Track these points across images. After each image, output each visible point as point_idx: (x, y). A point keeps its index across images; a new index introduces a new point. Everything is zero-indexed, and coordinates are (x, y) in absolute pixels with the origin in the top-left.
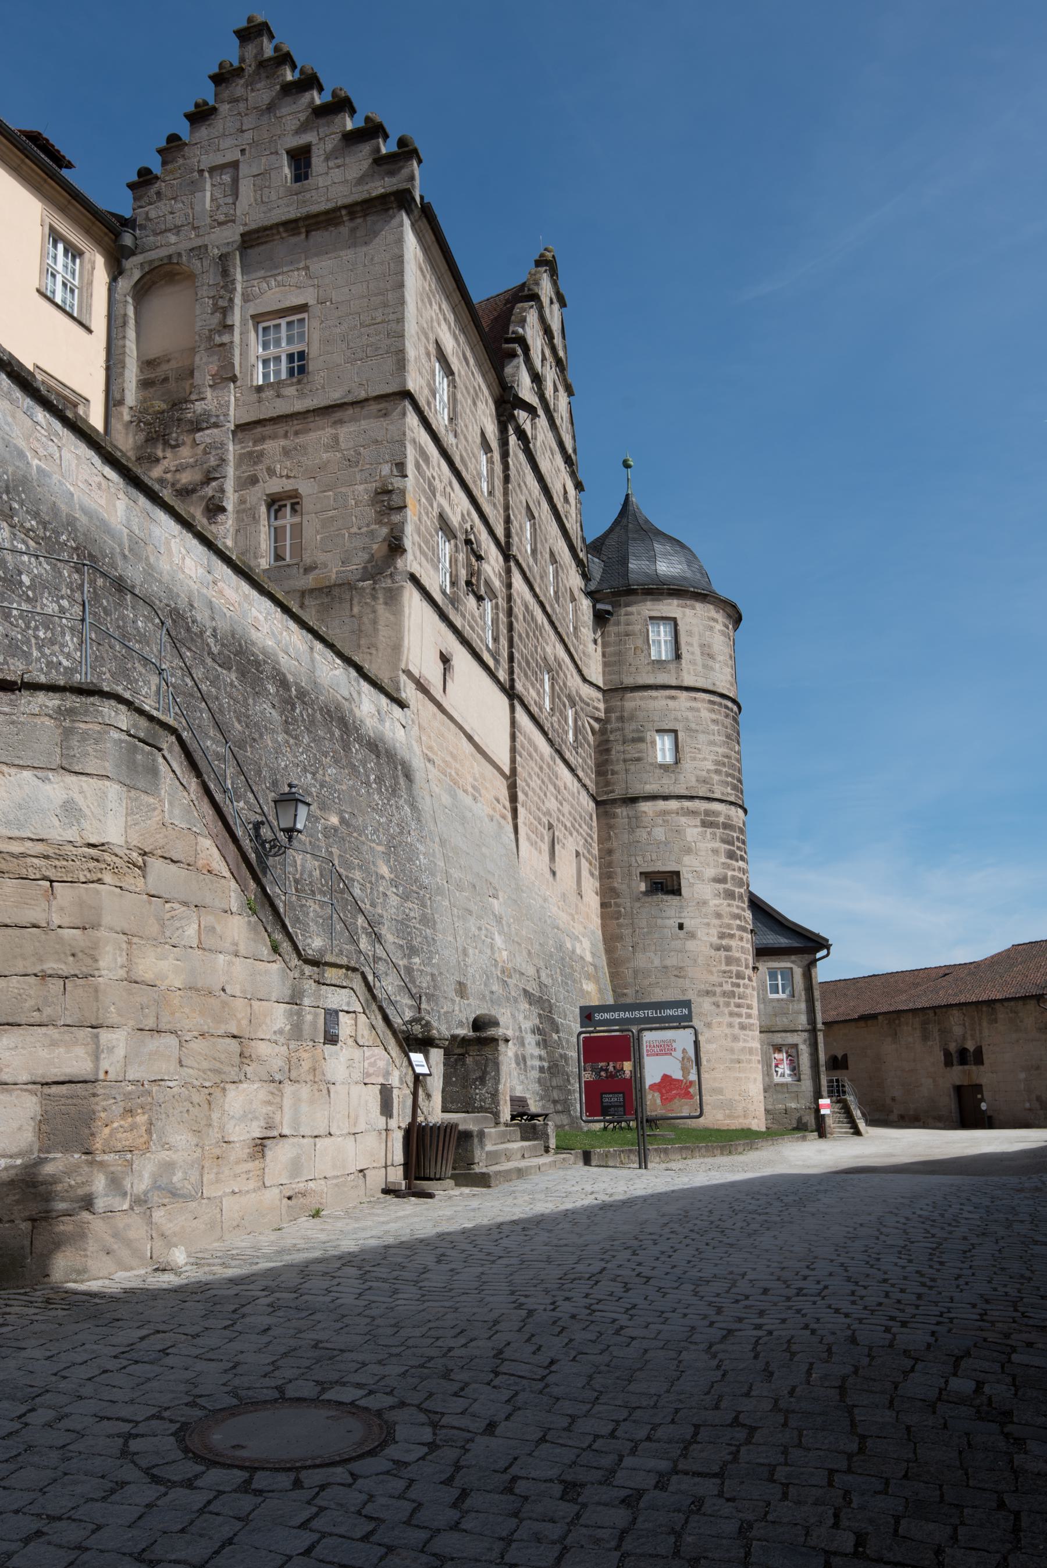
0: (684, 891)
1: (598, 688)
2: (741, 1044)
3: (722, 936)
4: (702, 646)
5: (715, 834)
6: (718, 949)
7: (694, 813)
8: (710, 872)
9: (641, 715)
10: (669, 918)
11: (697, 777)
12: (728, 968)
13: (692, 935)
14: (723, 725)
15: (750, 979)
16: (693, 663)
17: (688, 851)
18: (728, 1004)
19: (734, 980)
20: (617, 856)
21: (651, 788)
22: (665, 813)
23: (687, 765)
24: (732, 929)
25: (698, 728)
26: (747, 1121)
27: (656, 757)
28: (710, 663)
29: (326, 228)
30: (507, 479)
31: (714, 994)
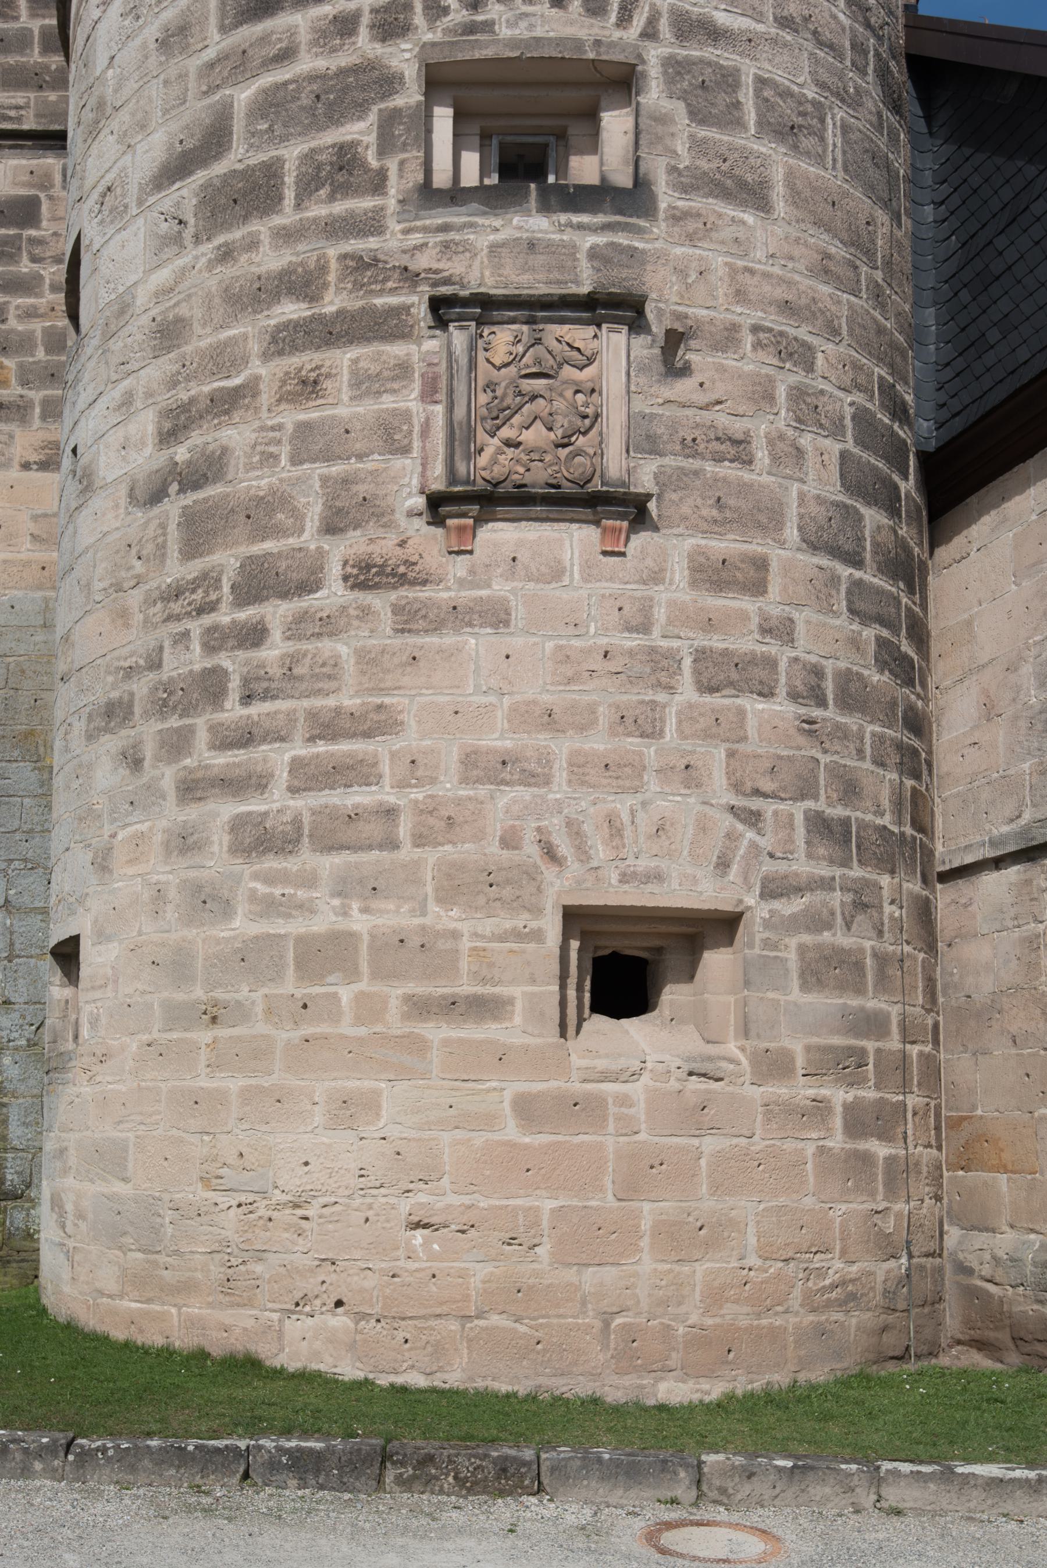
6: (157, 496)
12: (195, 568)
18: (177, 745)
19: (224, 617)
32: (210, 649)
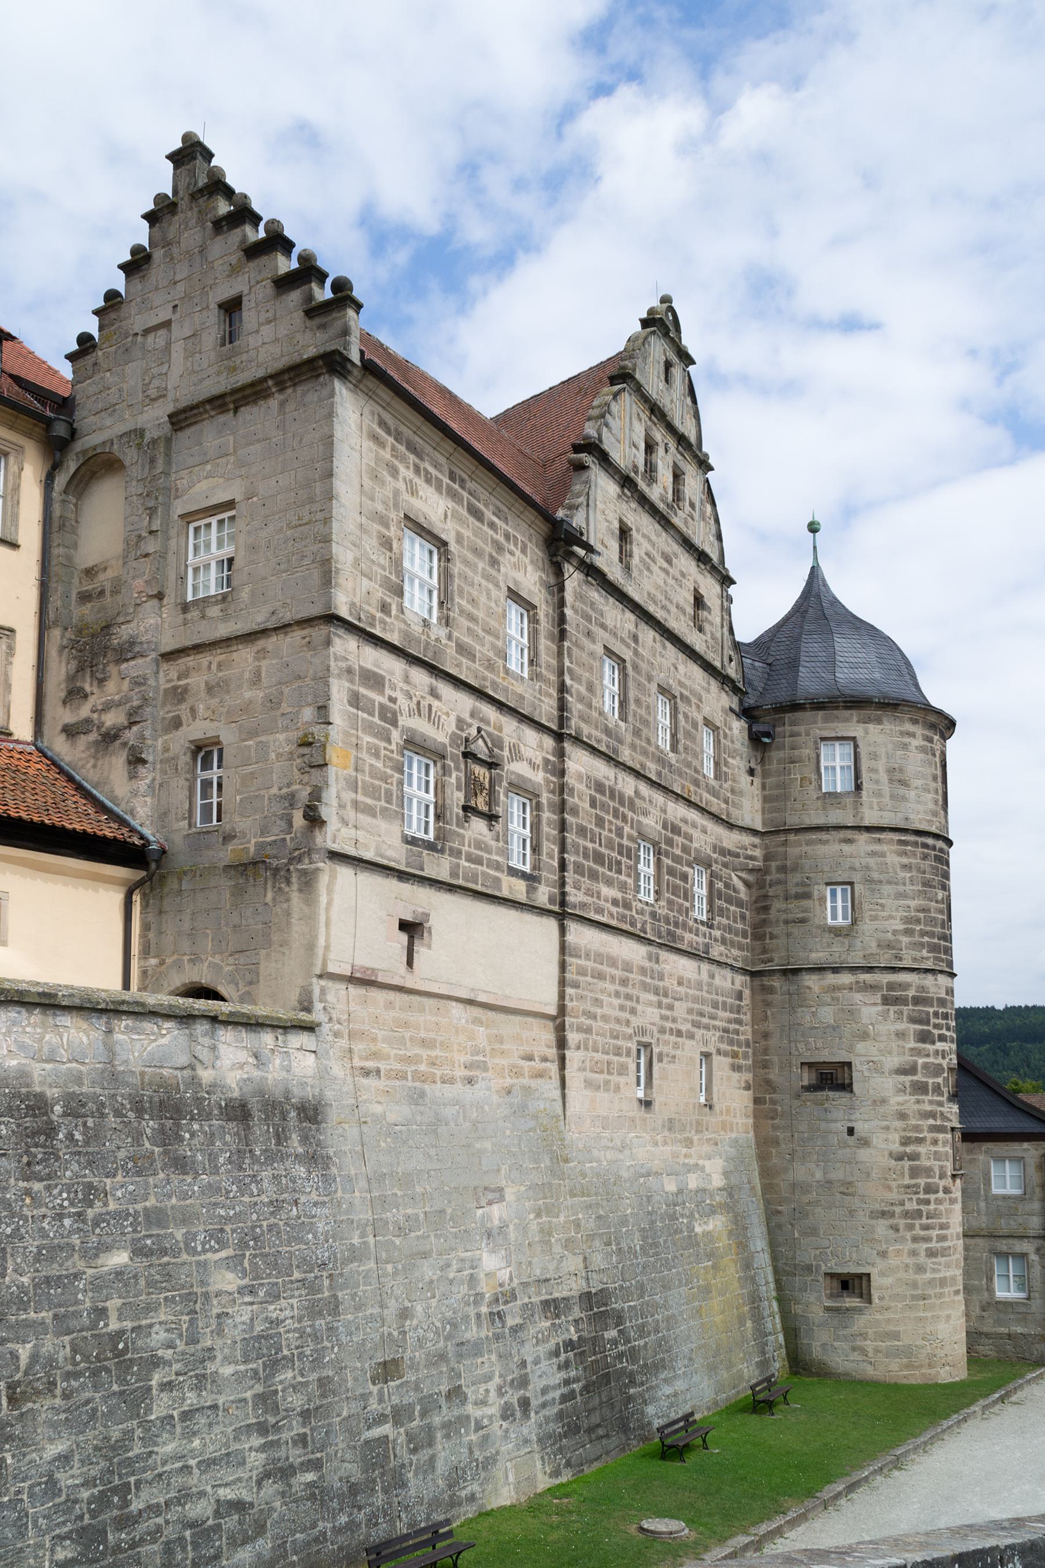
0: (855, 1087)
1: (754, 832)
2: (929, 1275)
3: (906, 1142)
4: (891, 771)
5: (902, 1013)
7: (873, 988)
8: (894, 1061)
9: (807, 863)
10: (836, 1121)
11: (879, 941)
12: (913, 1182)
13: (865, 1143)
14: (919, 870)
15: (947, 1191)
16: (878, 794)
17: (864, 1036)
18: (911, 1227)
19: (922, 1196)
20: (773, 1042)
21: (818, 956)
22: (835, 988)
23: (867, 926)
24: (922, 1131)
25: (882, 877)
26: (933, 1371)
27: (825, 918)
28: (902, 791)
29: (255, 402)
30: (562, 635)
31: (892, 1215)
32: (918, 1204)
